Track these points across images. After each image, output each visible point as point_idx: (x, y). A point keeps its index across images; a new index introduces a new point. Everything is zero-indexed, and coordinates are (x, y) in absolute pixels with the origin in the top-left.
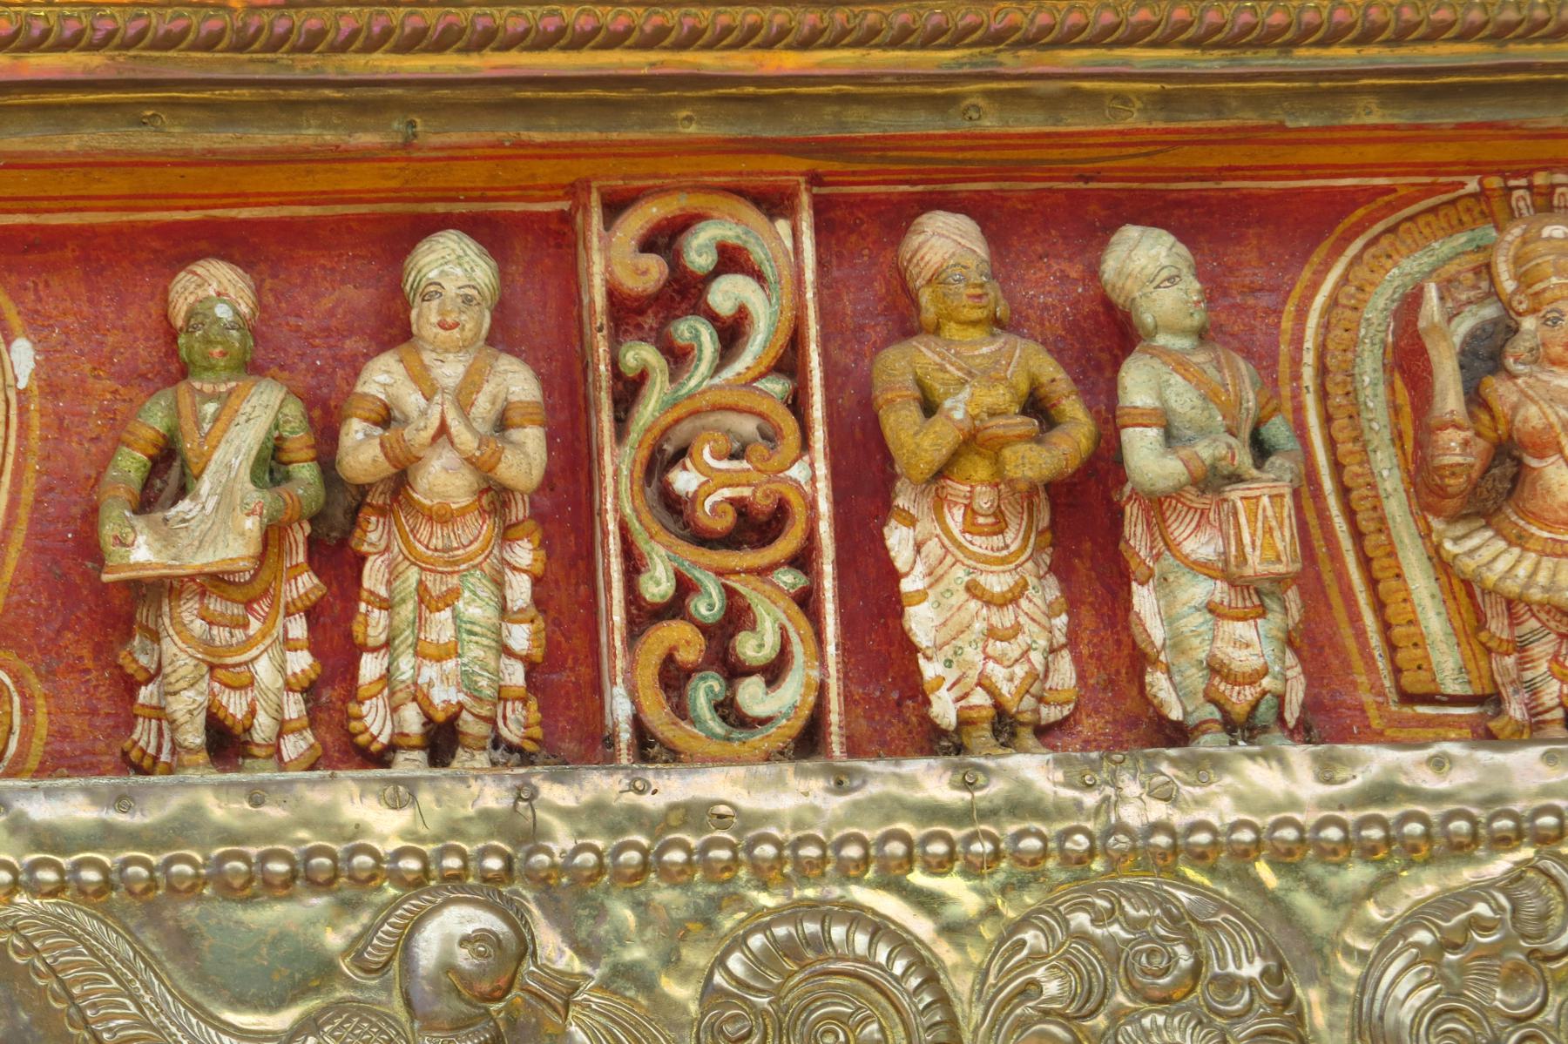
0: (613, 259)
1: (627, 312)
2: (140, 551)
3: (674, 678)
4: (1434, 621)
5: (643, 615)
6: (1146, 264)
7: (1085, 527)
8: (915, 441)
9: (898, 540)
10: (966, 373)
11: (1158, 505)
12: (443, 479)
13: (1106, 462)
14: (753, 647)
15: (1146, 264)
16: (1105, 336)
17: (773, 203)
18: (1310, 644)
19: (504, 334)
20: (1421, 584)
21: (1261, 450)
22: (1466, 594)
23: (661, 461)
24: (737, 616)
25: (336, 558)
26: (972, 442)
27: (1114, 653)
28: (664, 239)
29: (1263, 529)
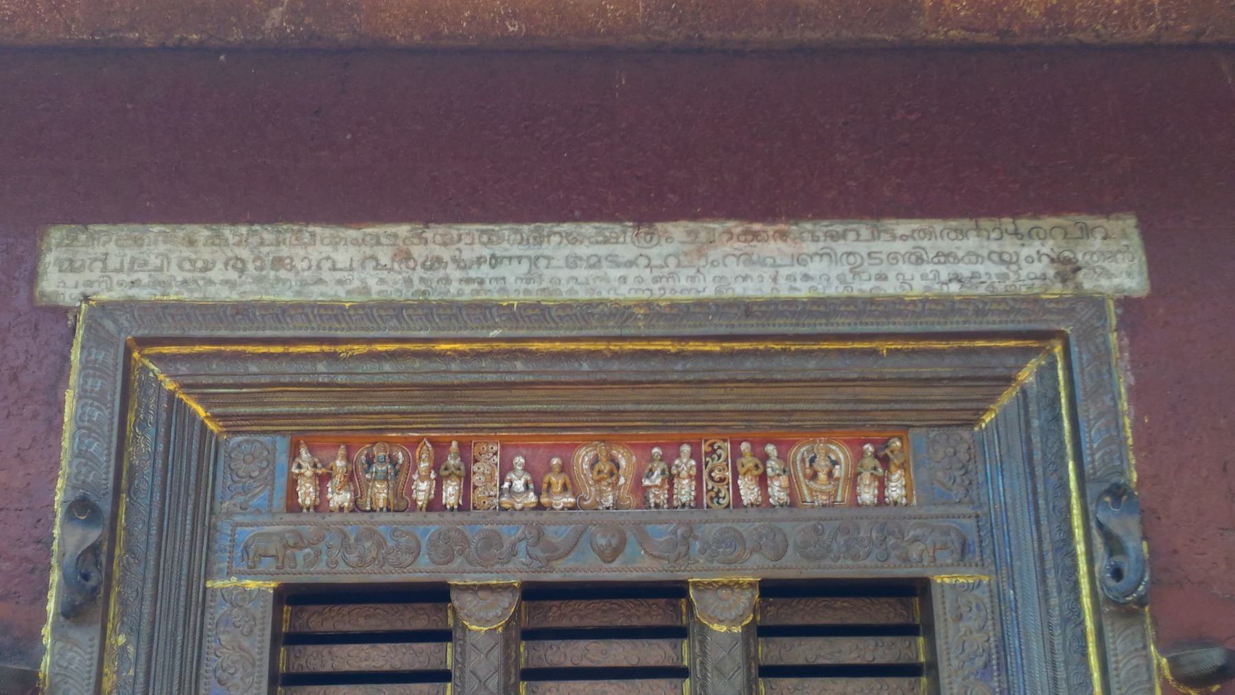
0: (705, 448)
1: (707, 454)
2: (646, 482)
3: (712, 499)
4: (806, 492)
5: (708, 491)
6: (771, 449)
7: (763, 480)
8: (741, 470)
9: (739, 482)
10: (748, 461)
11: (772, 478)
12: (684, 474)
13: (765, 472)
14: (721, 495)
15: (771, 449)
16: (765, 458)
17: (725, 441)
18: (790, 495)
19: (692, 456)
20: (804, 488)
21: (784, 471)
22: (811, 490)
23: (711, 471)
24: (719, 491)
25: (671, 484)
26: (748, 470)
27: (766, 496)
28: (712, 445)
29: (784, 480)
